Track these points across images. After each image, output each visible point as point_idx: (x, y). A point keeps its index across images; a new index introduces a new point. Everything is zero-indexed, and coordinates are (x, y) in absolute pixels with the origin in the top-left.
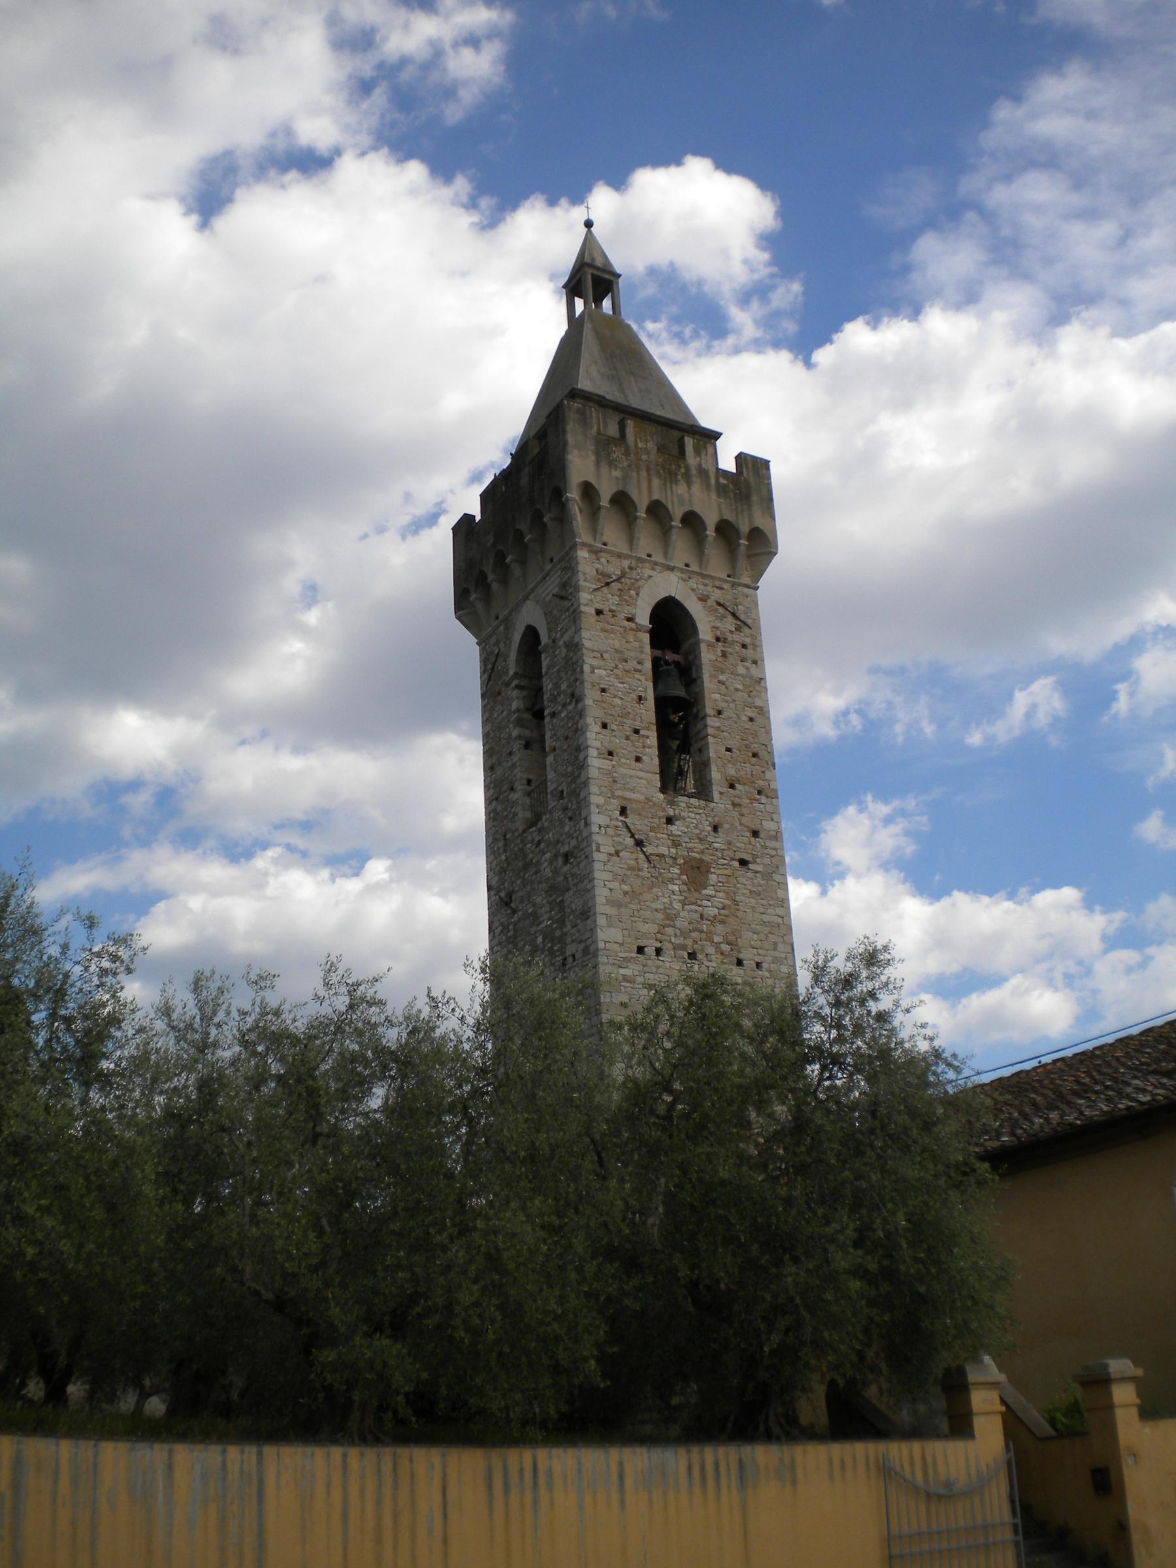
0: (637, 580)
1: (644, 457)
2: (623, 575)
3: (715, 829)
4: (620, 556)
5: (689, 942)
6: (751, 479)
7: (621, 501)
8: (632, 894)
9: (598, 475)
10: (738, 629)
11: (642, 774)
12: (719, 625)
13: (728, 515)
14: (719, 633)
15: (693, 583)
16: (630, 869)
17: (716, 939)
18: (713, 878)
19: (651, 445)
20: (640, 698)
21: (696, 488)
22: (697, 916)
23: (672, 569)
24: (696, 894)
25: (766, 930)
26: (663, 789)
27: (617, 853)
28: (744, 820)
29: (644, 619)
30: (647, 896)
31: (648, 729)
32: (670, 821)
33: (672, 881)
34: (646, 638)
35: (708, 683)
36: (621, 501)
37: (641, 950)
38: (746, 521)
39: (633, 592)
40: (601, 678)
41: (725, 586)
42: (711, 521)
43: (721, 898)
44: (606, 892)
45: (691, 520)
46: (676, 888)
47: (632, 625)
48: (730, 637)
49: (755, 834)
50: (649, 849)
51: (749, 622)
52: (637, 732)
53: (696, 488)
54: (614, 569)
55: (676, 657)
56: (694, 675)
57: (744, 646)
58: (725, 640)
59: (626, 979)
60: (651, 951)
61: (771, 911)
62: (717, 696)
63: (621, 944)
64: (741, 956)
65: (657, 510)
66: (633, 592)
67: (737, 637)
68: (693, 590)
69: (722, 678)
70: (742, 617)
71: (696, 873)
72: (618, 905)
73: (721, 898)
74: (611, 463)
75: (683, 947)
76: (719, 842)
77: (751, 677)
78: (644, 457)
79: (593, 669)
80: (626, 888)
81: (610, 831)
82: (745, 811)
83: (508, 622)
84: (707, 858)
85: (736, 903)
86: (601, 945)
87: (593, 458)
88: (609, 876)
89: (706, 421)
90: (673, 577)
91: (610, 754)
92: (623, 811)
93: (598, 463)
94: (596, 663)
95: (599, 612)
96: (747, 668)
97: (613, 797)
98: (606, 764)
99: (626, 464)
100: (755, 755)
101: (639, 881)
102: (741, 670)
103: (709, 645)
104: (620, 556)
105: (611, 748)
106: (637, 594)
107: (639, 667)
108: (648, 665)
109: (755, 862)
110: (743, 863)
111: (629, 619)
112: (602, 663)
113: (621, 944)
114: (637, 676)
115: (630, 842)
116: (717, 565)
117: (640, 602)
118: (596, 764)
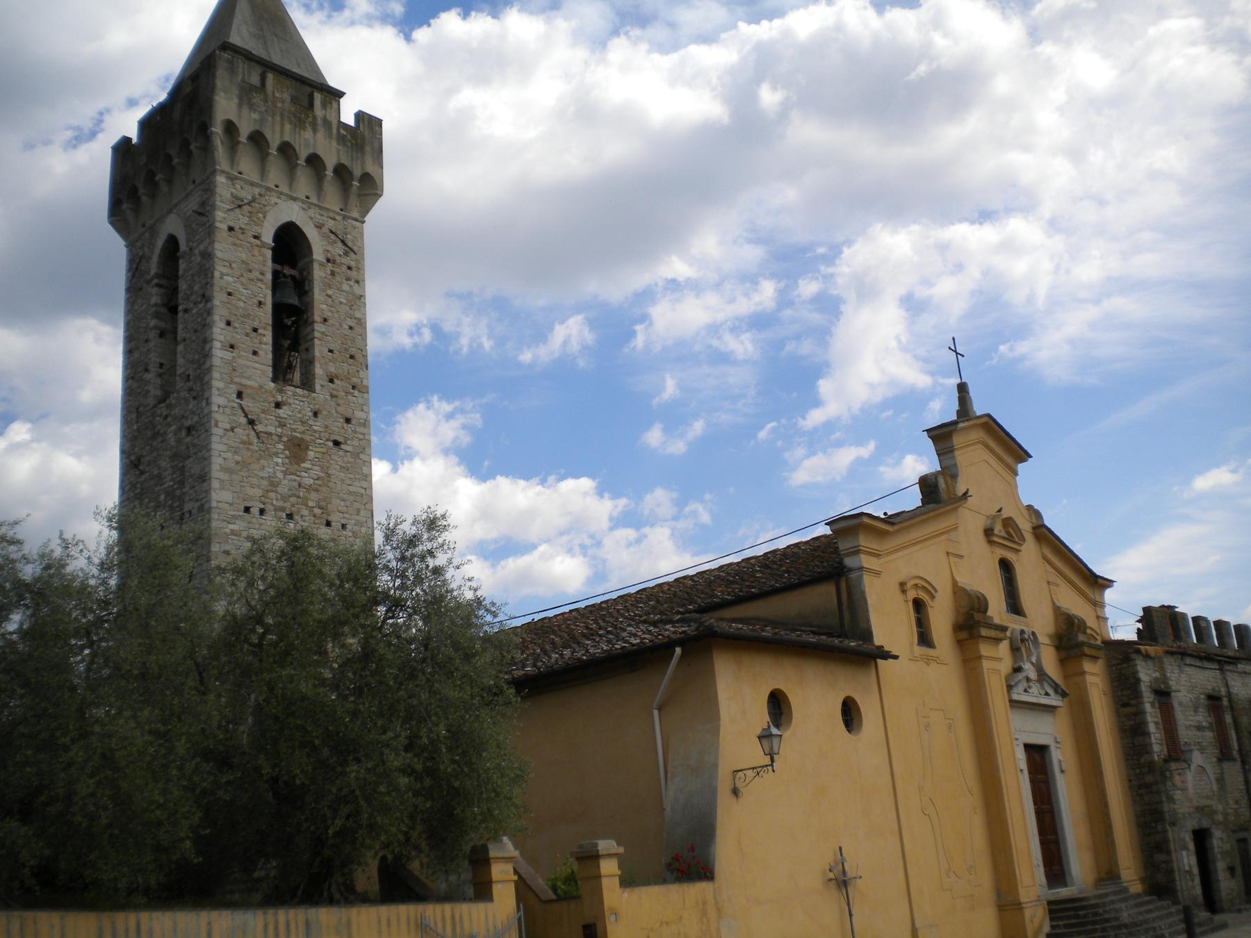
1: (279, 105)
3: (316, 414)
4: (252, 184)
5: (288, 505)
7: (257, 139)
8: (243, 464)
9: (240, 117)
10: (346, 254)
11: (257, 365)
13: (345, 161)
15: (311, 212)
16: (243, 443)
17: (311, 504)
18: (311, 454)
19: (287, 97)
20: (260, 303)
21: (321, 135)
22: (296, 484)
23: (294, 199)
24: (296, 467)
25: (352, 498)
26: (274, 379)
27: (232, 429)
28: (340, 409)
29: (268, 238)
30: (255, 466)
32: (278, 405)
33: (276, 454)
34: (269, 254)
35: (318, 295)
37: (247, 510)
38: (278, 135)
40: (228, 283)
42: (330, 162)
43: (317, 471)
44: (220, 461)
45: (314, 161)
46: (280, 460)
47: (258, 242)
48: (338, 260)
49: (348, 421)
50: (259, 428)
51: (355, 249)
52: (255, 330)
53: (321, 135)
54: (247, 194)
55: (294, 272)
56: (307, 288)
57: (349, 268)
58: (334, 262)
59: (233, 533)
60: (255, 511)
61: (357, 483)
62: (324, 307)
63: (231, 504)
64: (330, 519)
65: (286, 150)
67: (344, 260)
69: (330, 292)
70: (350, 244)
71: (297, 449)
72: (230, 471)
73: (317, 471)
74: (252, 107)
75: (282, 509)
76: (317, 425)
77: (353, 294)
78: (279, 105)
79: (222, 275)
80: (238, 458)
81: (228, 411)
82: (340, 401)
83: (153, 231)
84: (307, 438)
85: (329, 476)
86: (214, 504)
87: (236, 100)
88: (224, 448)
89: (333, 82)
91: (232, 347)
92: (240, 395)
93: (240, 106)
94: (225, 270)
95: (231, 229)
97: (232, 382)
98: (228, 355)
99: (263, 109)
100: (352, 357)
101: (249, 453)
102: (345, 287)
103: (321, 264)
104: (252, 184)
105: (233, 342)
108: (269, 276)
109: (346, 443)
110: (337, 443)
111: (256, 237)
112: (230, 272)
113: (231, 504)
114: (259, 284)
115: (243, 420)
116: (332, 199)
117: (266, 224)
118: (219, 354)
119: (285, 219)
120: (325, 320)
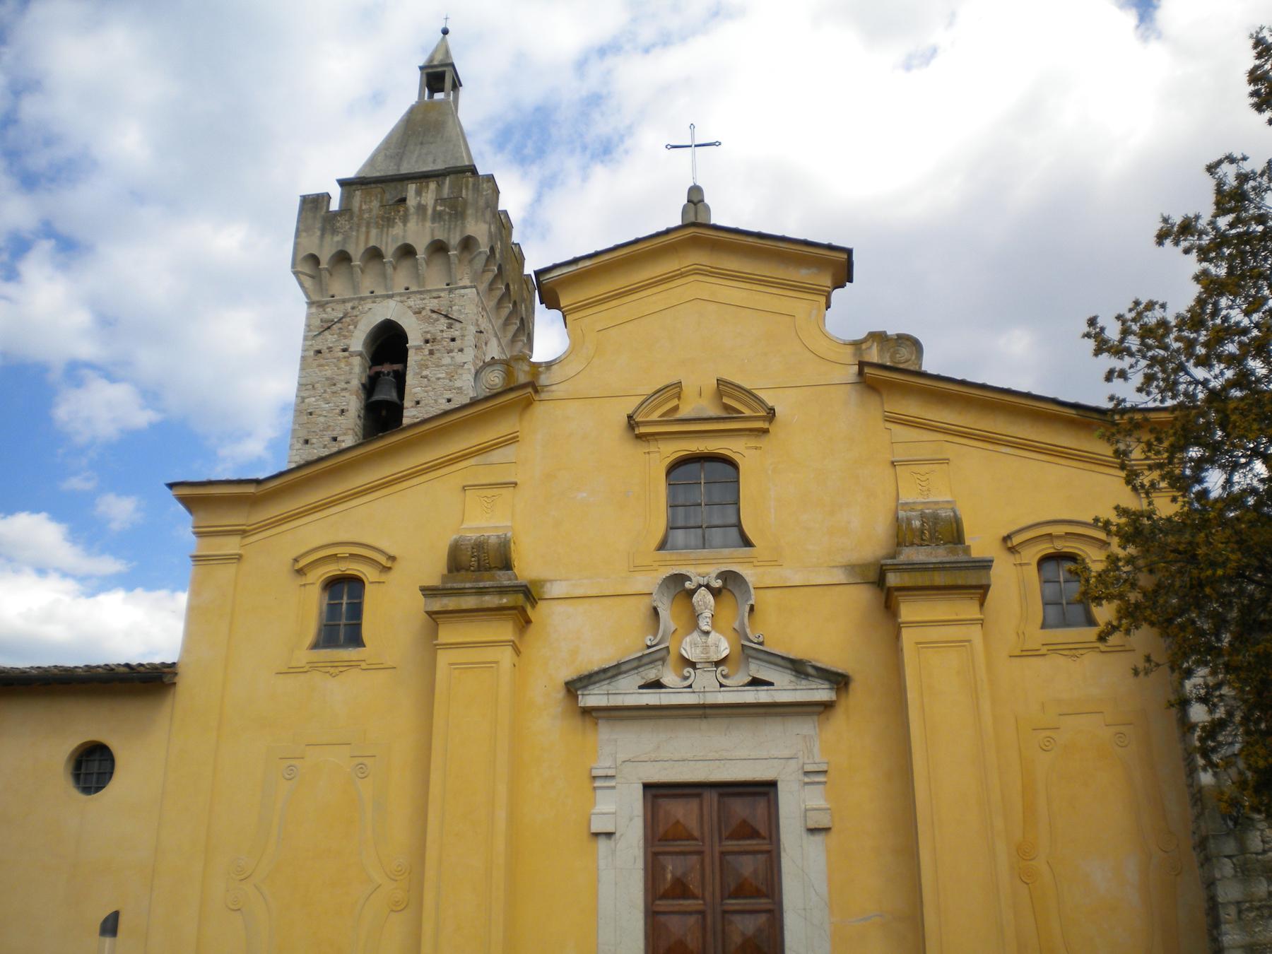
2: (345, 315)
6: (470, 196)
10: (450, 326)
13: (440, 236)
14: (429, 336)
19: (375, 204)
21: (412, 224)
23: (391, 297)
35: (410, 379)
36: (342, 258)
39: (351, 327)
40: (309, 405)
41: (442, 294)
45: (407, 252)
47: (346, 354)
51: (461, 317)
58: (434, 340)
65: (375, 254)
66: (351, 327)
68: (410, 307)
69: (424, 373)
87: (318, 233)
90: (392, 303)
95: (319, 352)
103: (418, 348)
104: (344, 301)
111: (344, 350)
119: (379, 319)
120: (418, 403)
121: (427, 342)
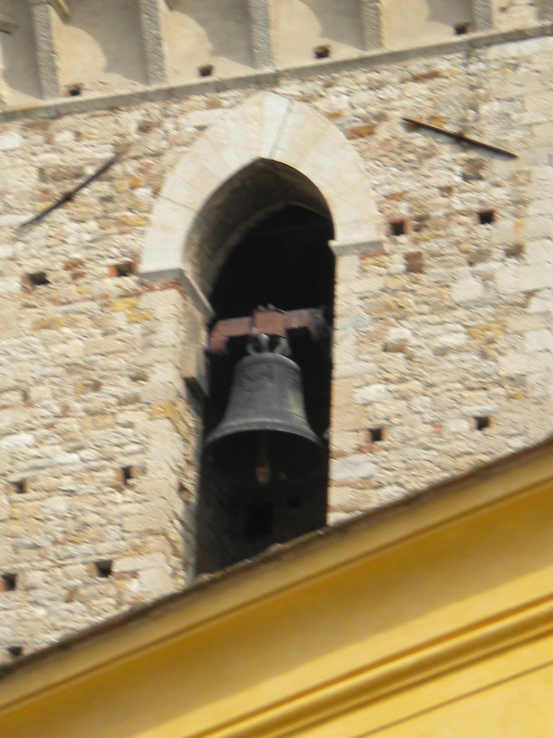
0: (157, 155)
12: (406, 184)
15: (336, 100)
31: (137, 550)
39: (143, 193)
47: (129, 282)
51: (511, 140)
58: (422, 222)
69: (394, 334)
95: (39, 279)
96: (486, 279)
102: (467, 287)
103: (369, 251)
106: (156, 193)
107: (134, 388)
111: (123, 270)
112: (22, 415)
120: (376, 435)
121: (398, 228)
